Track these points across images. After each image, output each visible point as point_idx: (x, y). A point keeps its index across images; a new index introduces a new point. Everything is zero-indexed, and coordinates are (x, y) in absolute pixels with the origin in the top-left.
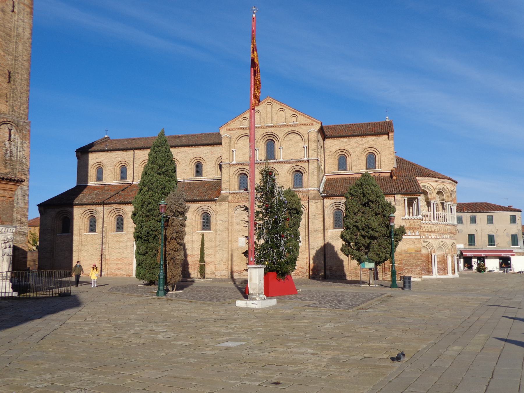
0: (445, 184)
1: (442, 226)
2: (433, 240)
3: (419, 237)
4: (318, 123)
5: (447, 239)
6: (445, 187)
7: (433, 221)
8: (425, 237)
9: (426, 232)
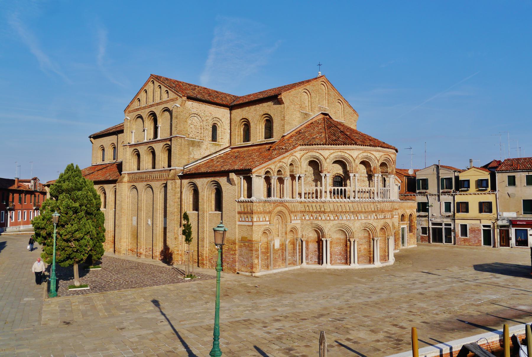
0: (346, 151)
1: (339, 204)
2: (324, 222)
3: (251, 224)
4: (180, 97)
5: (349, 220)
6: (346, 155)
7: (323, 199)
9: (315, 212)
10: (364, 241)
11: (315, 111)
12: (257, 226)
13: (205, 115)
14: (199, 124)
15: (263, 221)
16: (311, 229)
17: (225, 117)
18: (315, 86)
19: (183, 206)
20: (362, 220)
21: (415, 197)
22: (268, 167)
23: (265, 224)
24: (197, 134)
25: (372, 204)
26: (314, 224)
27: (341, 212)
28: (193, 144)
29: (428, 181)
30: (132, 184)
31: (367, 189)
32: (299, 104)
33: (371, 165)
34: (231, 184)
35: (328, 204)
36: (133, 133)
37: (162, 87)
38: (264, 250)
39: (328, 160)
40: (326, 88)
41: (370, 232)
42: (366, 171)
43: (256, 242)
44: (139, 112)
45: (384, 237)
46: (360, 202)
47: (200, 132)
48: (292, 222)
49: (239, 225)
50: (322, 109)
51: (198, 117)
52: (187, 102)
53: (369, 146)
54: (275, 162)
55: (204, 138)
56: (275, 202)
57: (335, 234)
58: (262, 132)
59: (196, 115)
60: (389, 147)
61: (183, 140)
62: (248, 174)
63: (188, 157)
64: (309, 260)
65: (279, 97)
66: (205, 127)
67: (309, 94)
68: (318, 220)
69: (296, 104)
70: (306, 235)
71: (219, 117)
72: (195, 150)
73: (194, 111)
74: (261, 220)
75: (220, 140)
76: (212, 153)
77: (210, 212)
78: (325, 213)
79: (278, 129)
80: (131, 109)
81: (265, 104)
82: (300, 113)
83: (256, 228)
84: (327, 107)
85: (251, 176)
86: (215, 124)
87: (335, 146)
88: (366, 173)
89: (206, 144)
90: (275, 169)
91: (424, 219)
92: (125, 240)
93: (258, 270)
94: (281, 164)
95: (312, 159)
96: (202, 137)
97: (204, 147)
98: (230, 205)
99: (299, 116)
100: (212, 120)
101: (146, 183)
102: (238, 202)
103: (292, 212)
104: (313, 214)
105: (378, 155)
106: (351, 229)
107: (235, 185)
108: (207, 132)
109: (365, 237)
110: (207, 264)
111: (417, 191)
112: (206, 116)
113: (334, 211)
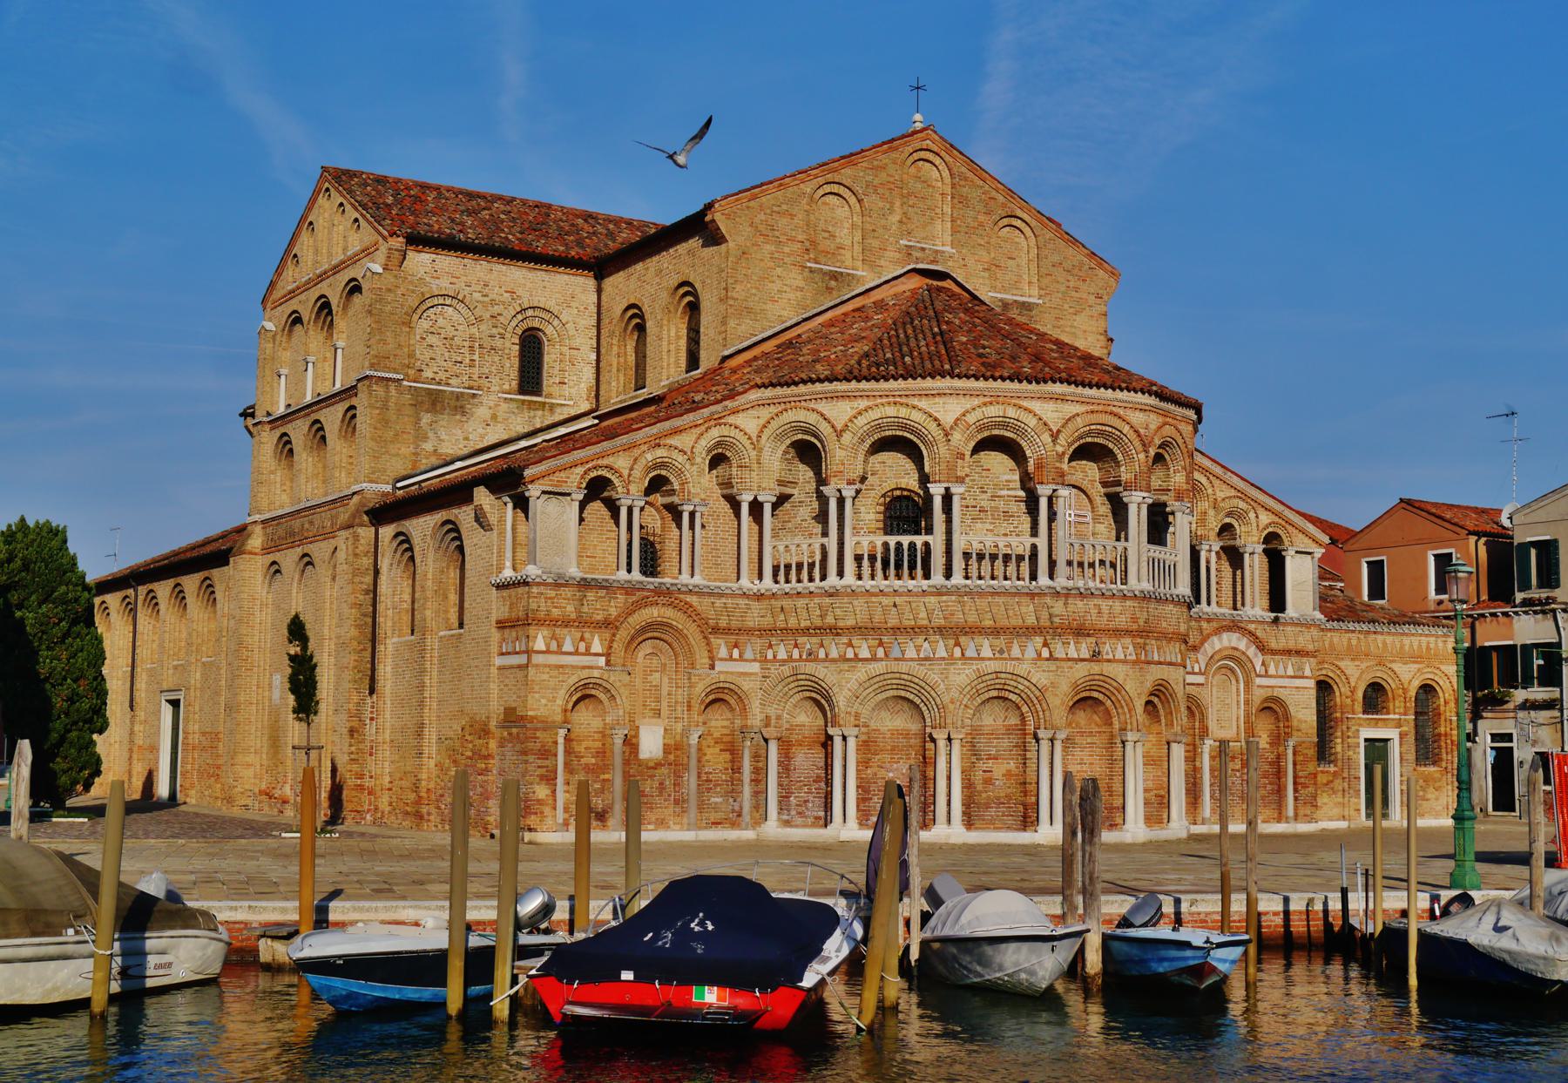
0: (915, 402)
1: (886, 601)
2: (833, 667)
3: (522, 659)
4: (384, 238)
5: (926, 659)
6: (916, 416)
7: (832, 579)
8: (801, 656)
9: (806, 631)
10: (1006, 743)
11: (882, 263)
12: (547, 670)
13: (486, 299)
14: (464, 332)
15: (576, 653)
16: (798, 697)
17: (572, 304)
18: (883, 168)
19: (382, 619)
20: (983, 659)
21: (1511, 623)
22: (600, 462)
23: (587, 664)
24: (457, 369)
25: (1026, 600)
26: (803, 677)
27: (896, 630)
28: (434, 404)
29: (1557, 548)
30: (271, 558)
31: (1021, 543)
32: (800, 238)
33: (1028, 453)
34: (483, 527)
35: (846, 600)
36: (283, 378)
37: (348, 207)
38: (593, 761)
39: (847, 438)
40: (946, 173)
41: (1025, 709)
42: (1017, 477)
43: (539, 725)
44: (293, 305)
45: (1105, 737)
46: (970, 593)
47: (467, 361)
48: (717, 668)
49: (500, 668)
50: (916, 254)
51: (460, 306)
52: (411, 254)
53: (1012, 380)
54: (634, 446)
55: (484, 382)
56: (629, 589)
57: (884, 714)
58: (678, 350)
59: (448, 302)
60: (1118, 379)
61: (393, 392)
62: (517, 488)
63: (412, 449)
64: (793, 813)
65: (708, 218)
66: (487, 343)
67: (853, 200)
68: (816, 660)
69: (783, 239)
70: (779, 718)
71: (550, 305)
72: (444, 423)
73: (444, 284)
74: (568, 647)
75: (555, 390)
76: (513, 435)
77: (442, 633)
78: (838, 634)
79: (712, 333)
80: (278, 293)
81: (682, 248)
82: (806, 273)
83: (545, 677)
84: (948, 249)
85: (527, 494)
86: (534, 332)
87: (872, 385)
88: (1018, 485)
89: (492, 404)
90: (631, 469)
91: (1543, 716)
92: (250, 759)
93: (549, 821)
94: (660, 452)
95: (800, 436)
96: (475, 377)
97: (482, 412)
98: (479, 600)
99: (801, 283)
100: (520, 317)
101: (299, 551)
102: (499, 587)
103: (716, 630)
104: (801, 640)
105: (1052, 413)
106: (934, 695)
107: (492, 529)
108: (497, 359)
109: (1009, 730)
110: (432, 818)
111: (1519, 597)
112: (493, 303)
113: (870, 625)
